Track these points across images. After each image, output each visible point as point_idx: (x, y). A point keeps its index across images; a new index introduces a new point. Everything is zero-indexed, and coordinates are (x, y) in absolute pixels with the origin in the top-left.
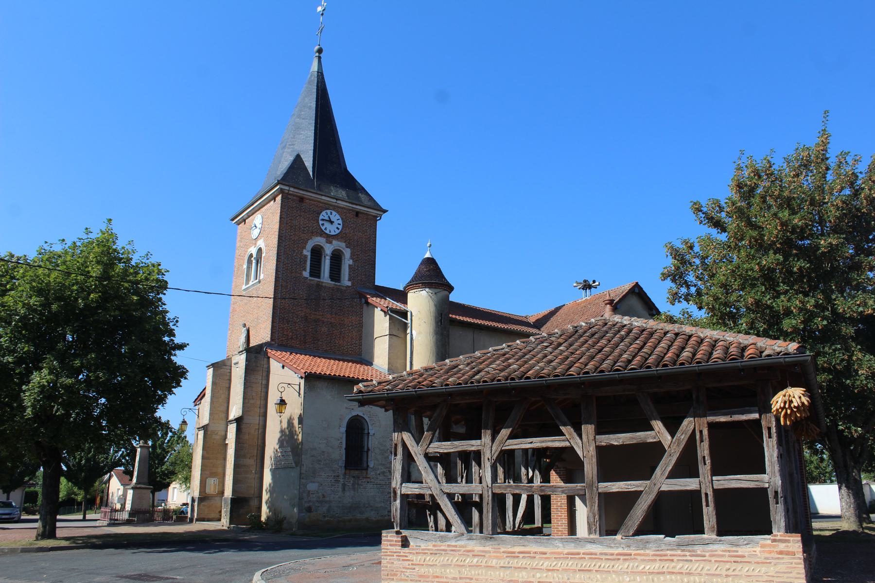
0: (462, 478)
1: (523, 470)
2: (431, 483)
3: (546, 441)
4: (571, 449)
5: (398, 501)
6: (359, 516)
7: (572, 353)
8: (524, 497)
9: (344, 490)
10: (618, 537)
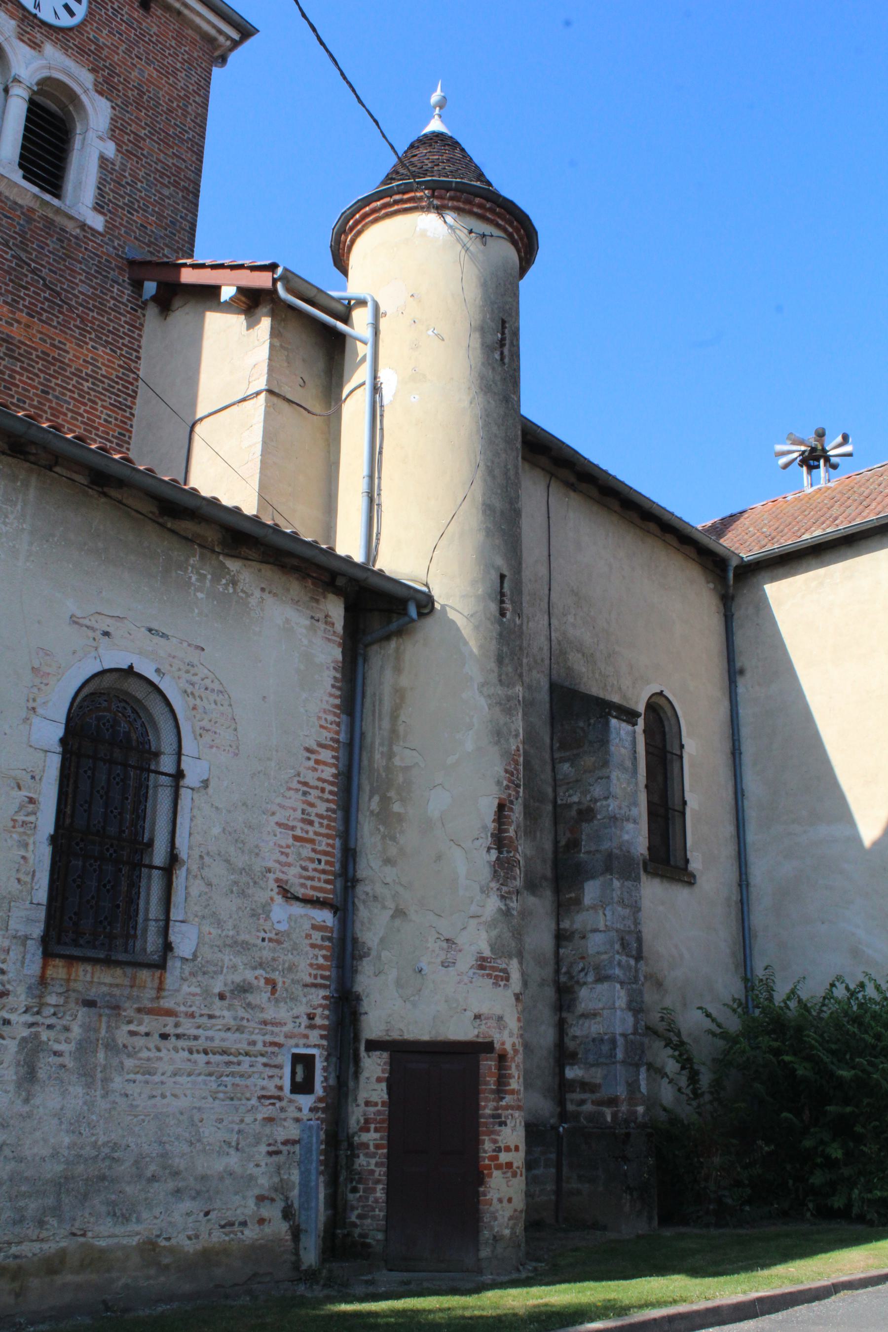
6: (106, 1234)
9: (29, 1076)
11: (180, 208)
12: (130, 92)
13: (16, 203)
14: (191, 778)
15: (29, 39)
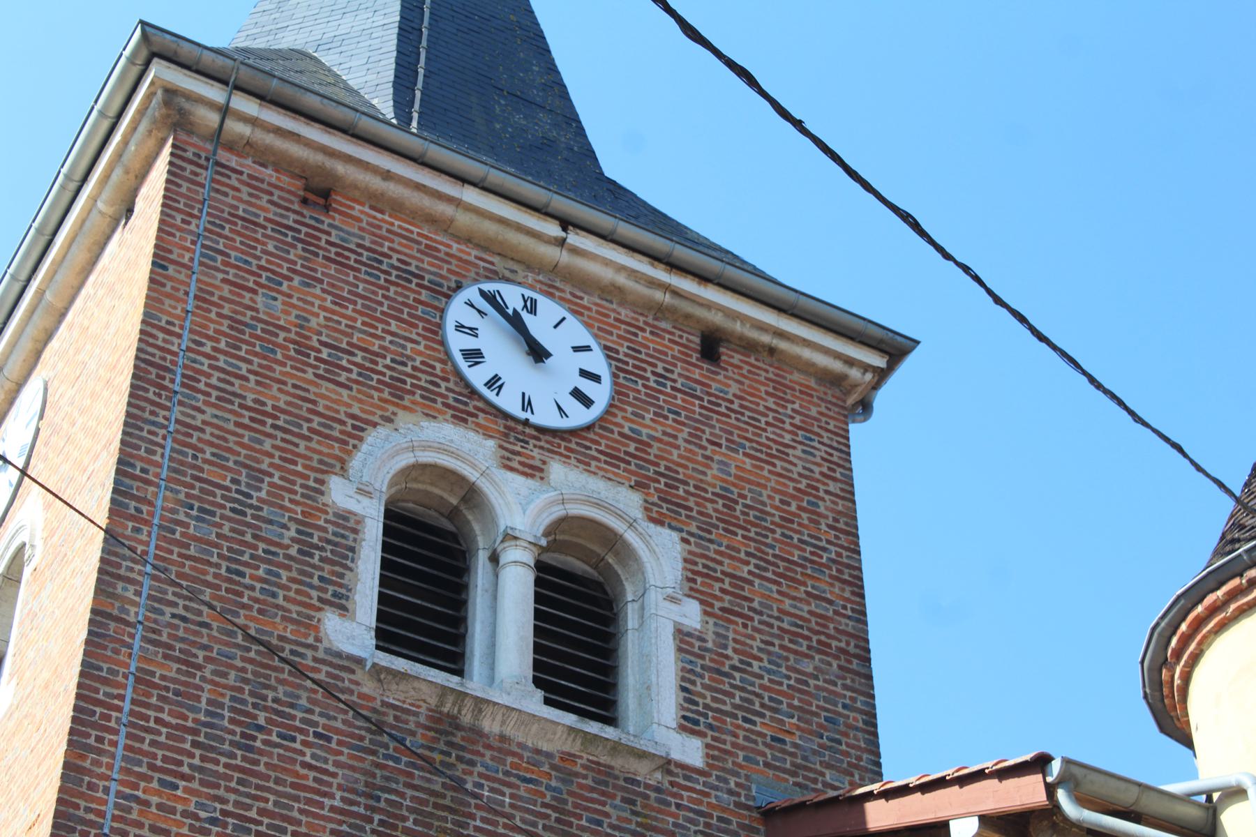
11: (839, 689)
12: (709, 505)
13: (538, 752)
15: (521, 463)
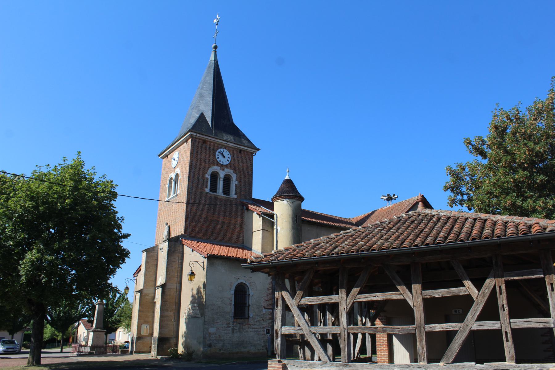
0: (321, 323)
1: (359, 318)
2: (301, 325)
3: (386, 295)
4: (404, 301)
5: (279, 339)
6: (243, 350)
7: (401, 234)
8: (360, 336)
9: (233, 332)
10: (441, 364)
14: (251, 295)
